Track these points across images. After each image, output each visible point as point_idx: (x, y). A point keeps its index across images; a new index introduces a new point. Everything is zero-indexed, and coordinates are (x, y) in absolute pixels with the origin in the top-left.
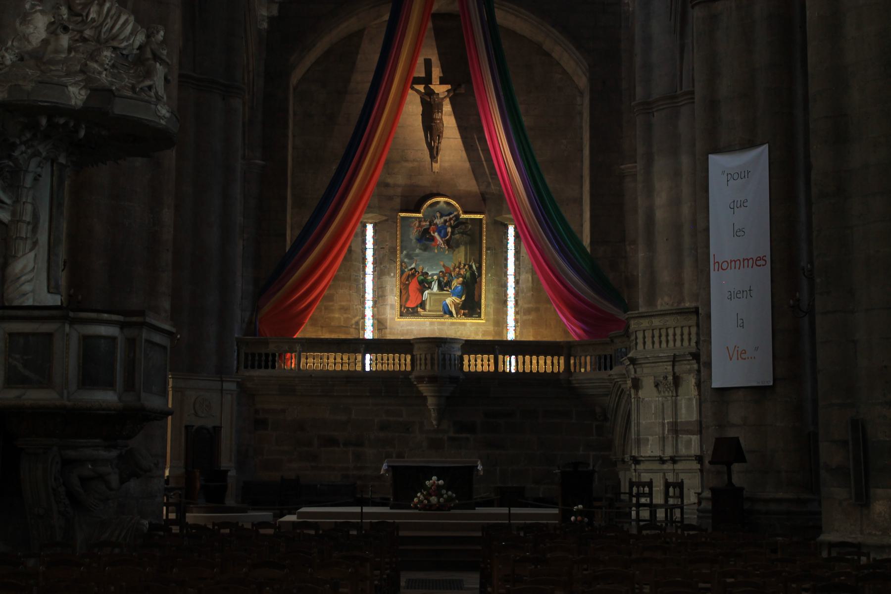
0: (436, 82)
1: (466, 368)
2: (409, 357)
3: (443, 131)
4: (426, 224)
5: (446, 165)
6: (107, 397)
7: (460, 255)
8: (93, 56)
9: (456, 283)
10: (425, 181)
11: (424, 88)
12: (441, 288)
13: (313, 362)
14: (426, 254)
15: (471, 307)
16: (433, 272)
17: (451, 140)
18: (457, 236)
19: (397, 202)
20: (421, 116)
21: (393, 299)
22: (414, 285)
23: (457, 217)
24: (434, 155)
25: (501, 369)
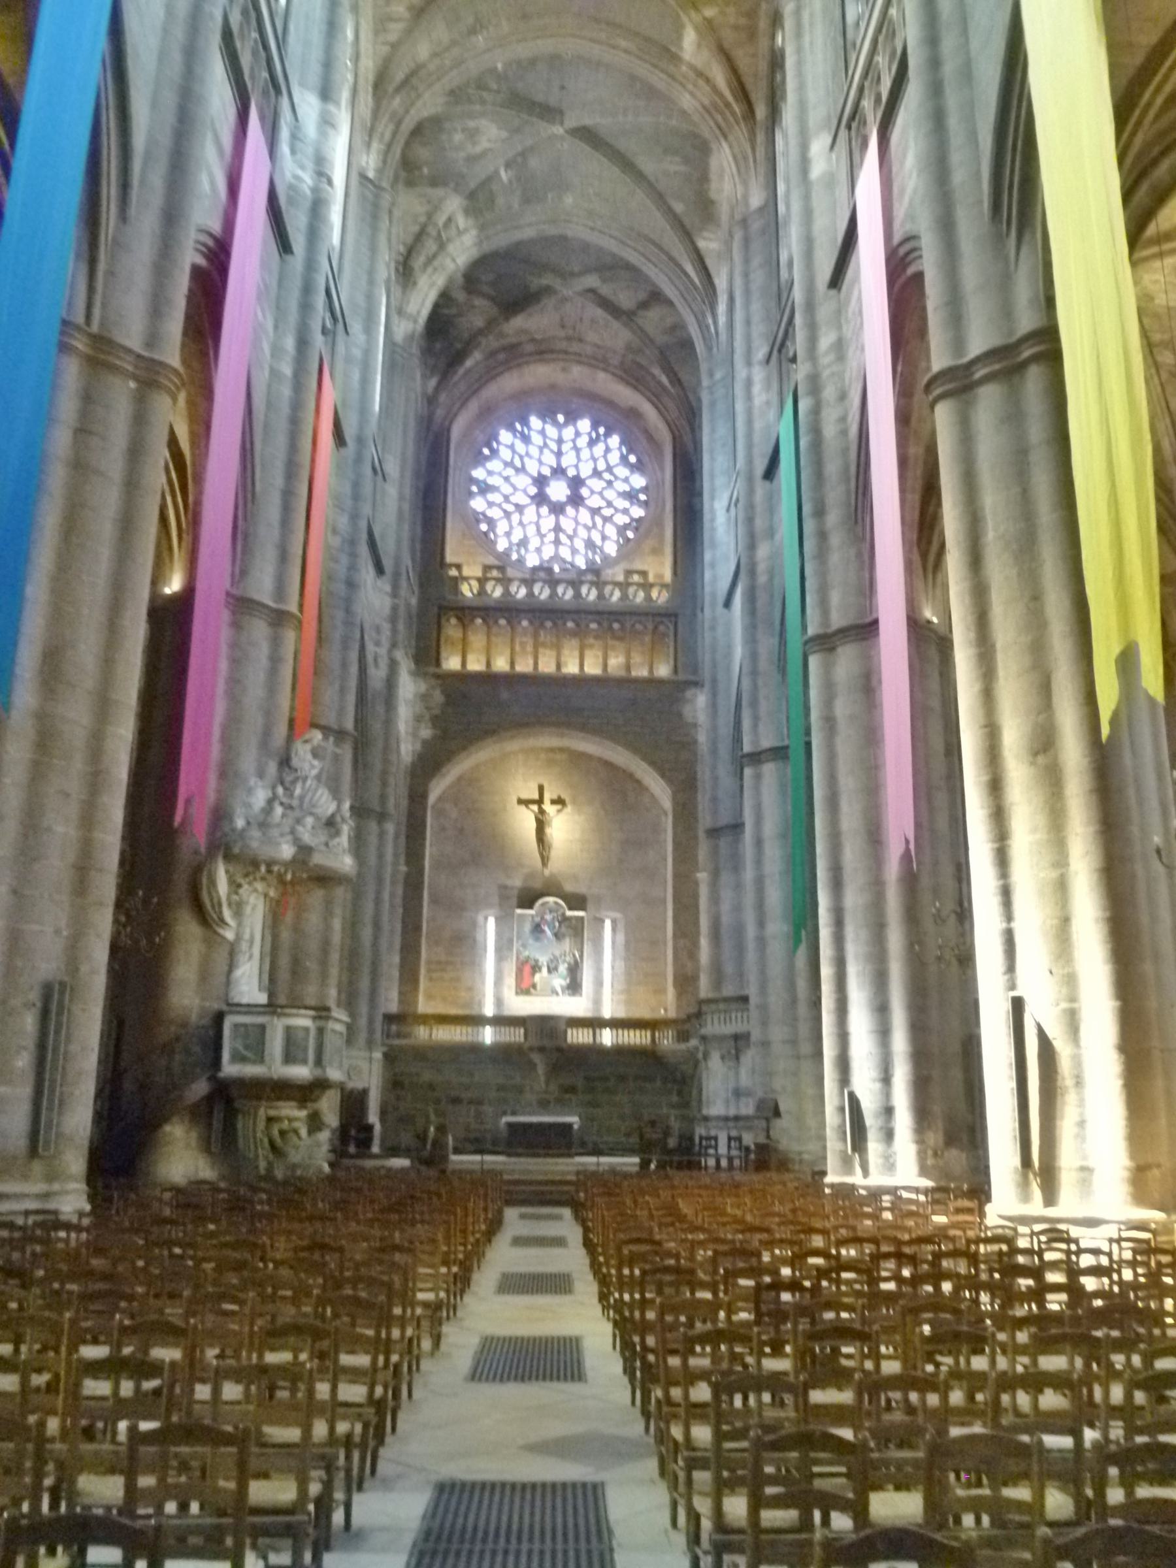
1: (569, 1040)
2: (522, 1031)
4: (538, 919)
5: (555, 871)
6: (301, 1072)
7: (567, 944)
8: (298, 821)
9: (563, 968)
10: (537, 885)
12: (549, 971)
13: (445, 1034)
14: (538, 944)
15: (574, 987)
16: (543, 960)
18: (563, 929)
19: (514, 901)
21: (510, 981)
22: (527, 969)
23: (563, 914)
25: (598, 1040)
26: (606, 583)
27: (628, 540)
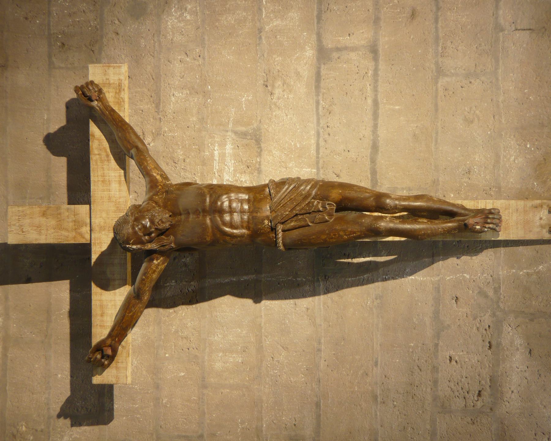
0: (78, 224)
3: (315, 183)
11: (106, 286)
17: (382, 132)
20: (265, 303)
24: (449, 231)
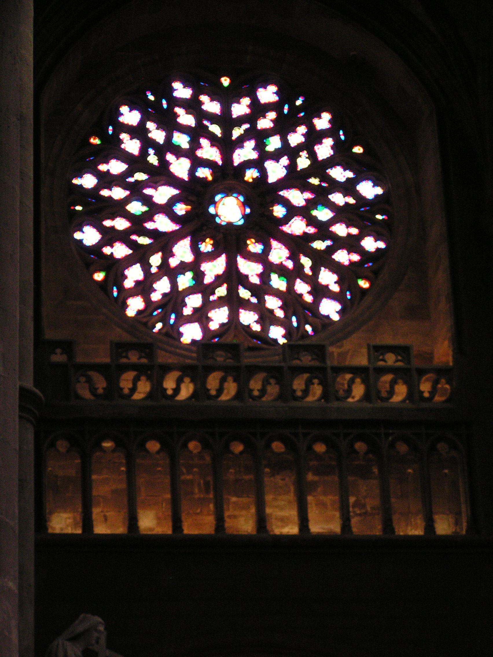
26: (338, 370)
27: (364, 291)
